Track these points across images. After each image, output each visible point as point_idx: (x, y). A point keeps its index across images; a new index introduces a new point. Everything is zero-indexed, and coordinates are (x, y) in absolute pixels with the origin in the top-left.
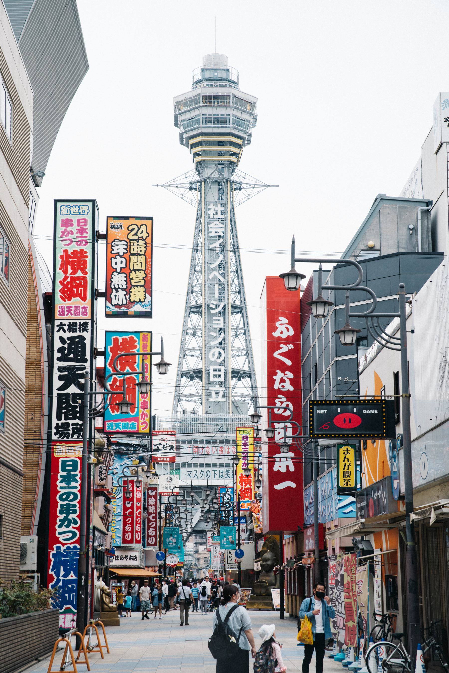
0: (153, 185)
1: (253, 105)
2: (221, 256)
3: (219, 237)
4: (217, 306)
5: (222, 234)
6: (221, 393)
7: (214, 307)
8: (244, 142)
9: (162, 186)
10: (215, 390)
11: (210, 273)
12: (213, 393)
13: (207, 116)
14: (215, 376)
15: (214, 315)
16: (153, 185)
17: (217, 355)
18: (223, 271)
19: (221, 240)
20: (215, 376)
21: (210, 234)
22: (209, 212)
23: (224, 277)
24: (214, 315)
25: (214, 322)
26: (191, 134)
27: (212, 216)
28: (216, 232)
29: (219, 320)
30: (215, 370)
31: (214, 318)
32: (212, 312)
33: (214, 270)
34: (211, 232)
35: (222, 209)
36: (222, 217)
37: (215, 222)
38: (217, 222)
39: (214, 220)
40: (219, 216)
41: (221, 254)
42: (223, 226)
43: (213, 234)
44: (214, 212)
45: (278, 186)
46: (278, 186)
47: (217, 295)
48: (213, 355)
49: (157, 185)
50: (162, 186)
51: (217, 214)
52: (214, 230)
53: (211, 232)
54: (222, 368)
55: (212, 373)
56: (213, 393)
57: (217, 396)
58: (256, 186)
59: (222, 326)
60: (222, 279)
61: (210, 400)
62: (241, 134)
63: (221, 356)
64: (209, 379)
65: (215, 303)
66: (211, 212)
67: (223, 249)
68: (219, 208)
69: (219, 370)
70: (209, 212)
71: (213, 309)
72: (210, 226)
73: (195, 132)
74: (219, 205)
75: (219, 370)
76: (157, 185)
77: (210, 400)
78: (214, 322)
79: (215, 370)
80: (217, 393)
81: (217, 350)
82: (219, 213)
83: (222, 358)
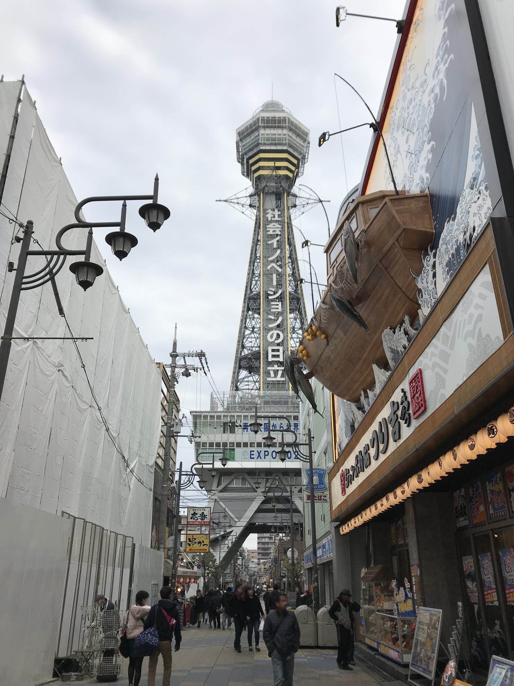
0: (216, 201)
1: (307, 134)
2: (279, 251)
3: (277, 235)
4: (275, 293)
5: (279, 233)
6: (280, 373)
7: (272, 293)
8: (298, 163)
9: (226, 201)
10: (273, 370)
11: (269, 265)
12: (272, 374)
13: (265, 136)
14: (273, 356)
15: (273, 300)
16: (216, 201)
17: (275, 336)
18: (280, 263)
19: (278, 238)
20: (273, 356)
21: (268, 233)
22: (267, 216)
23: (281, 268)
24: (273, 300)
25: (272, 307)
26: (251, 154)
27: (269, 219)
28: (274, 231)
29: (278, 305)
30: (273, 350)
31: (272, 303)
32: (270, 297)
33: (272, 261)
34: (269, 231)
35: (280, 213)
36: (280, 219)
37: (273, 224)
38: (275, 224)
39: (271, 222)
40: (277, 218)
41: (278, 248)
42: (280, 226)
43: (271, 233)
44: (272, 216)
45: (329, 201)
46: (329, 201)
47: (275, 283)
48: (272, 337)
50: (226, 201)
51: (274, 217)
52: (271, 230)
53: (269, 231)
54: (281, 348)
55: (270, 354)
56: (272, 374)
57: (276, 376)
58: (310, 201)
59: (280, 310)
60: (280, 270)
61: (269, 379)
62: (296, 154)
63: (279, 337)
64: (267, 359)
65: (273, 290)
66: (269, 216)
67: (280, 245)
68: (277, 213)
69: (278, 350)
70: (267, 216)
71: (271, 295)
72: (268, 226)
73: (255, 151)
74: (276, 211)
75: (278, 350)
76: (220, 201)
77: (269, 379)
78: (272, 307)
79: (273, 350)
80: (276, 372)
81: (275, 332)
82: (276, 216)
83: (280, 340)
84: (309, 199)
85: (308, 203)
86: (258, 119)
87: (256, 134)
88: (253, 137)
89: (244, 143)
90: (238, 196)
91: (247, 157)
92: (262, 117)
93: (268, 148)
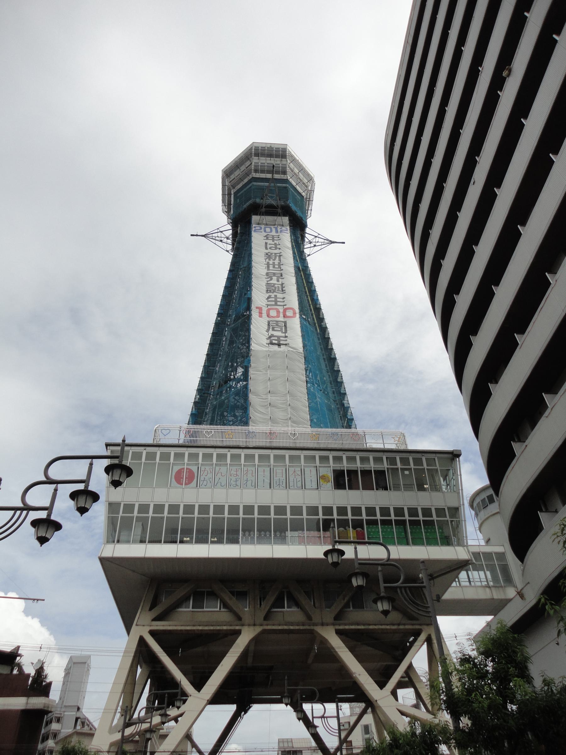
0: (192, 235)
16: (192, 235)
45: (344, 243)
46: (344, 243)
49: (197, 235)
76: (197, 235)
84: (316, 237)
85: (315, 246)
86: (251, 149)
87: (248, 163)
88: (243, 168)
89: (231, 180)
90: (221, 229)
91: (235, 190)
92: (255, 147)
93: (263, 176)
